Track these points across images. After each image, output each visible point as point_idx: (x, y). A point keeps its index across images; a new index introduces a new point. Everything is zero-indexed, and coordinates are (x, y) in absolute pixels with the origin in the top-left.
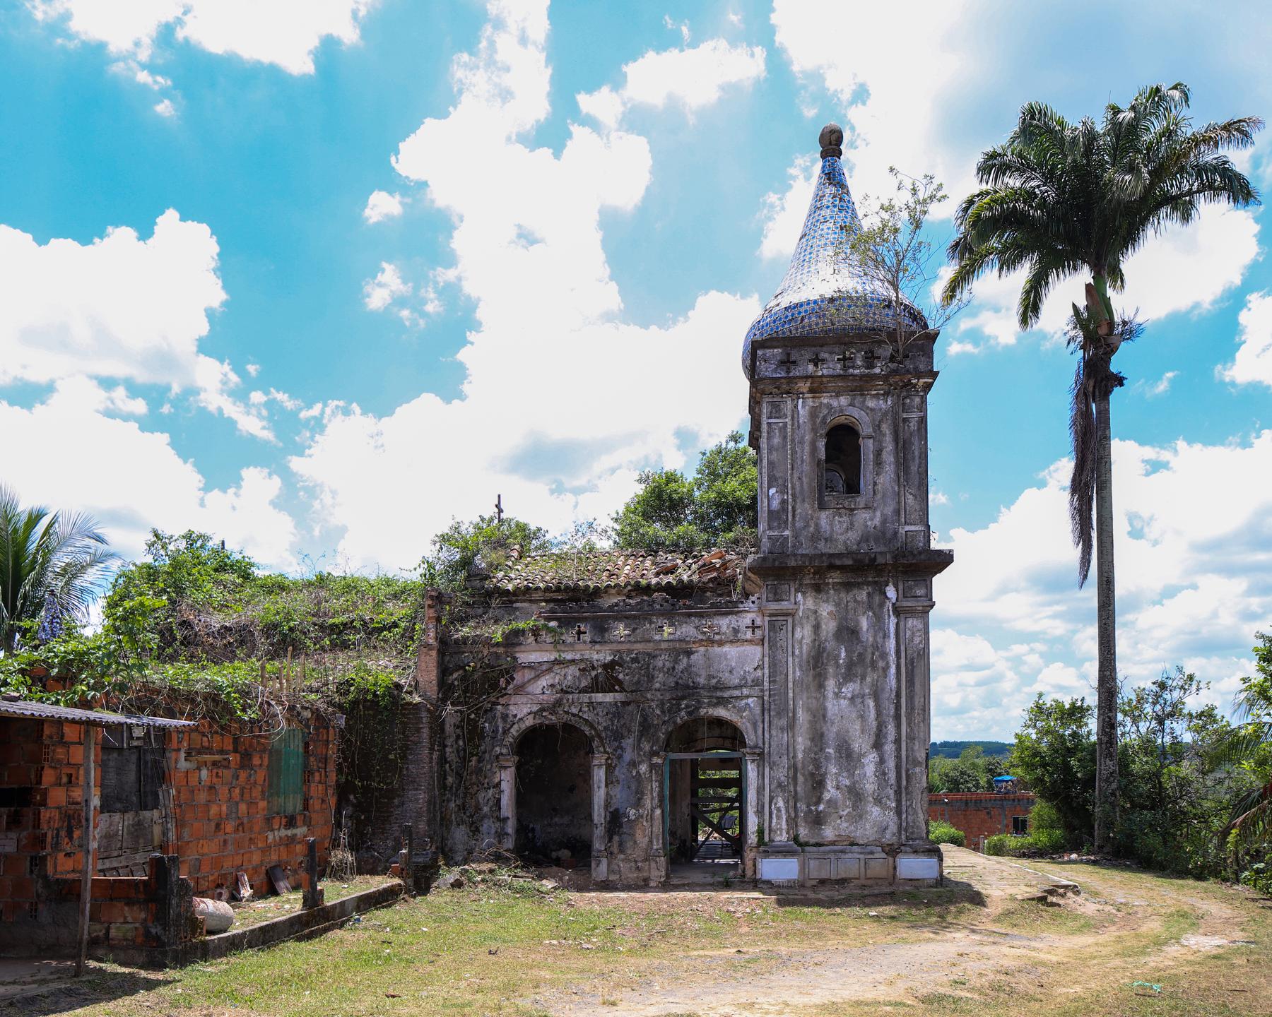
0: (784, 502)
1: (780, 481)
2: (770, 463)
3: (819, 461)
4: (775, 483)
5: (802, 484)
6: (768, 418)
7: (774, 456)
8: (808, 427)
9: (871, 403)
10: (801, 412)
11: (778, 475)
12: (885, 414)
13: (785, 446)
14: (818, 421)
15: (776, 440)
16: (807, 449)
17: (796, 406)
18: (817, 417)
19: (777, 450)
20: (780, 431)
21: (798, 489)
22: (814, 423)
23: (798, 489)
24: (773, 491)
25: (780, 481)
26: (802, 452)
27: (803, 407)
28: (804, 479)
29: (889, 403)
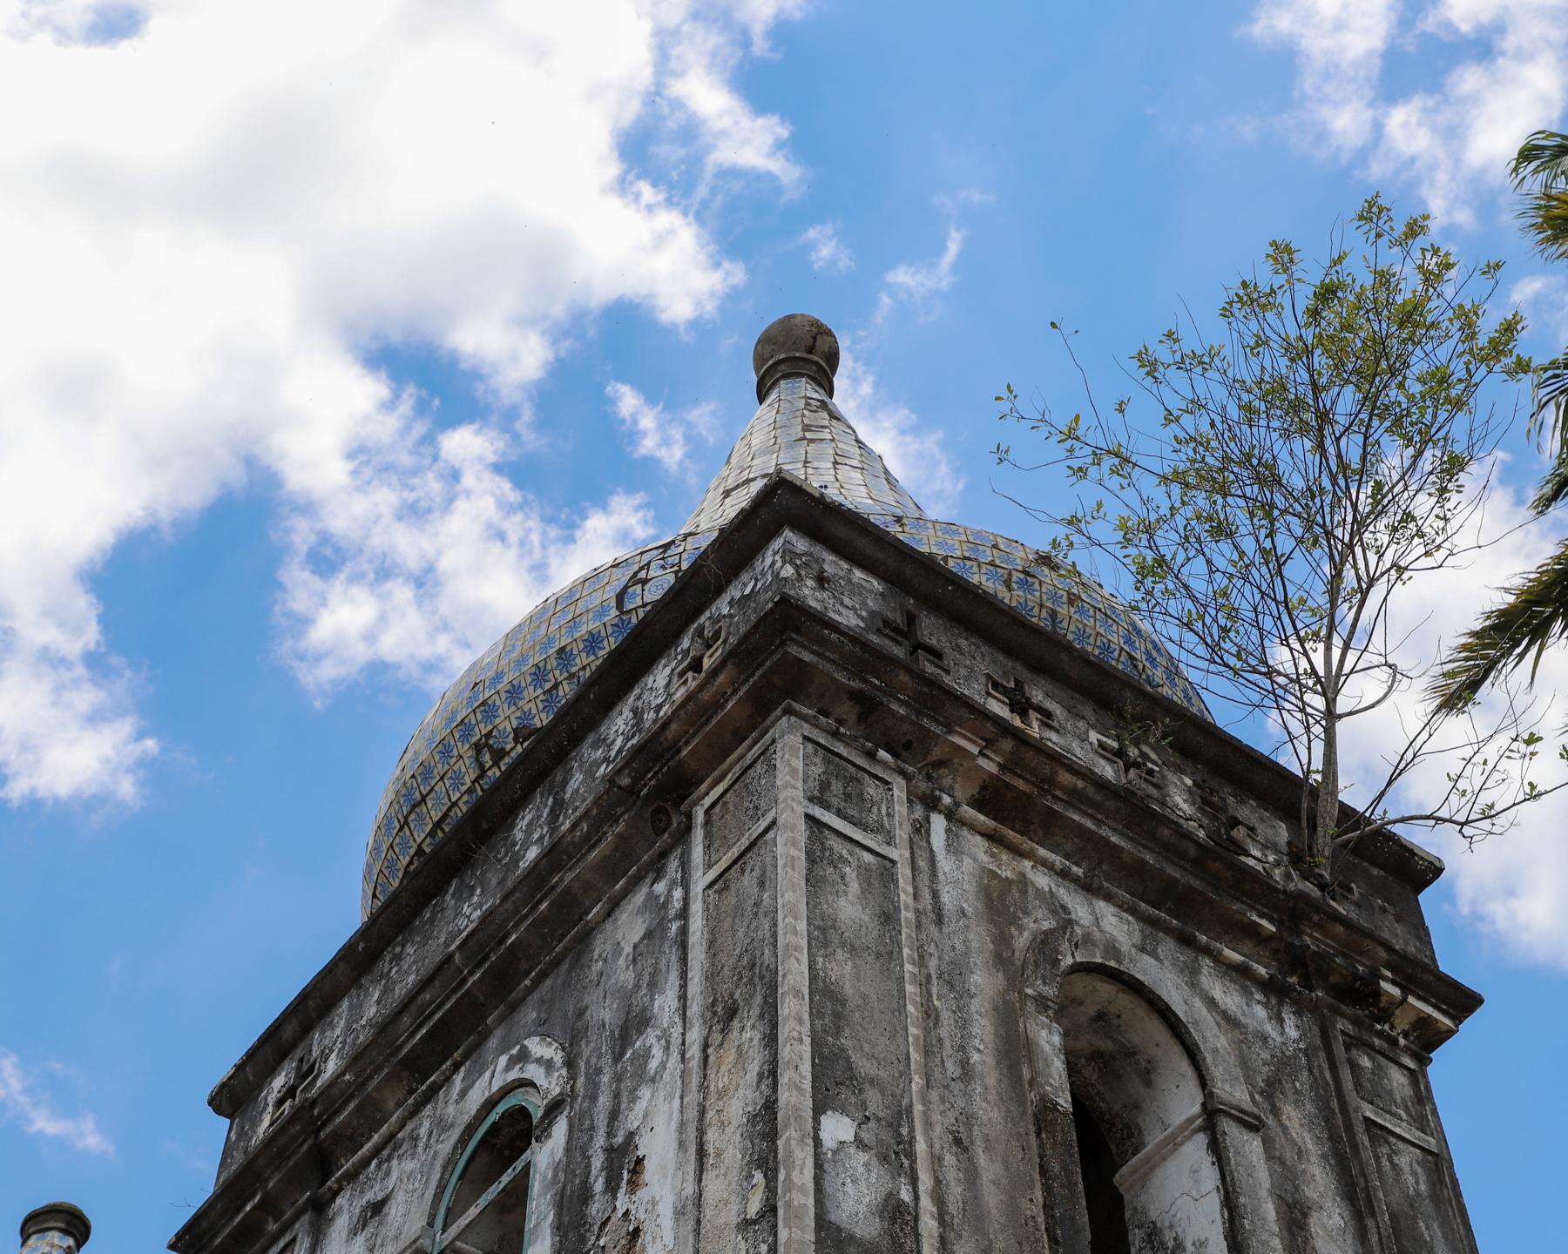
0: (897, 1214)
1: (875, 1101)
2: (823, 994)
3: (1047, 1107)
4: (845, 1094)
5: (971, 1175)
6: (827, 807)
7: (841, 969)
8: (978, 938)
9: (1229, 997)
10: (945, 864)
11: (864, 1067)
12: (1283, 1066)
13: (888, 955)
14: (1022, 941)
15: (850, 909)
16: (983, 1030)
17: (921, 830)
18: (1014, 921)
19: (854, 951)
20: (865, 872)
21: (955, 1192)
22: (1002, 940)
23: (955, 1192)
24: (837, 1128)
25: (875, 1101)
26: (963, 1024)
27: (953, 847)
28: (982, 1159)
29: (1293, 1033)
